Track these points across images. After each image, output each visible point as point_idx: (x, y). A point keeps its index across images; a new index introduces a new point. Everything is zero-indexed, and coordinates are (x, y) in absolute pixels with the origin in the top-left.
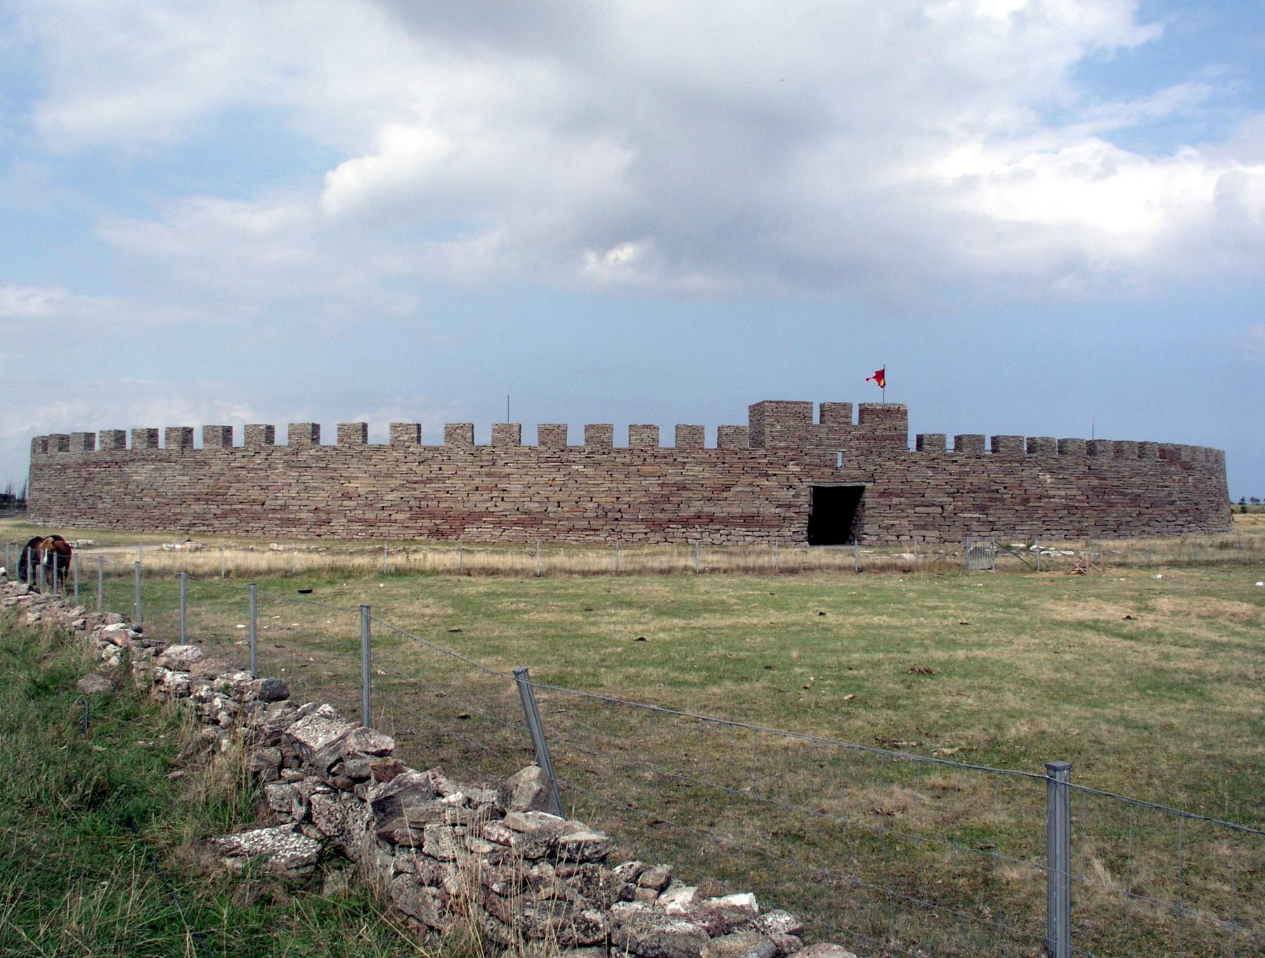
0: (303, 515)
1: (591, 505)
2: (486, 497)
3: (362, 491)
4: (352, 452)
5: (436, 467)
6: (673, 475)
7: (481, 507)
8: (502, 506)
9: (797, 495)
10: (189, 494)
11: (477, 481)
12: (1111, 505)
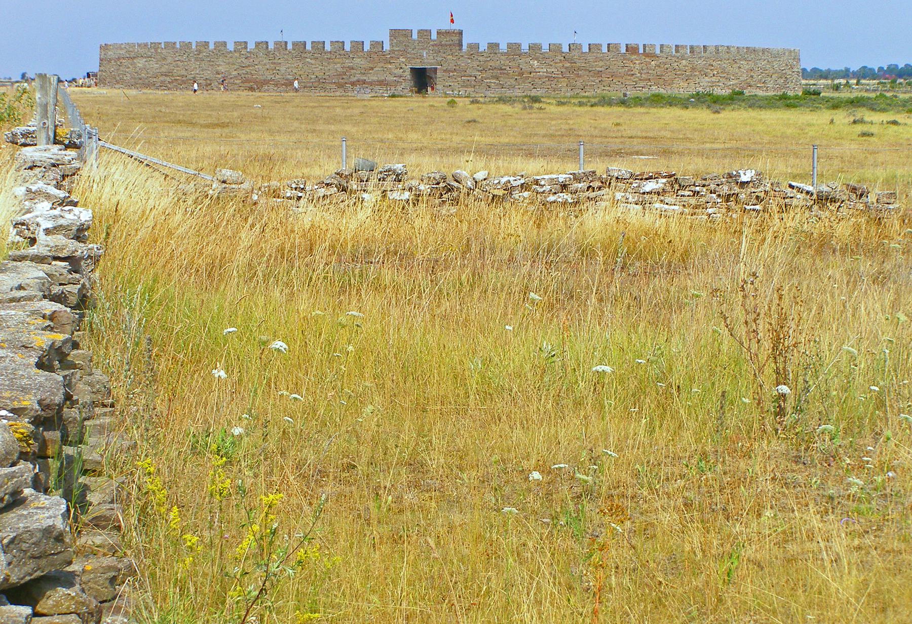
1: (313, 77)
6: (348, 63)
8: (277, 77)
9: (404, 72)
11: (268, 67)
12: (578, 76)
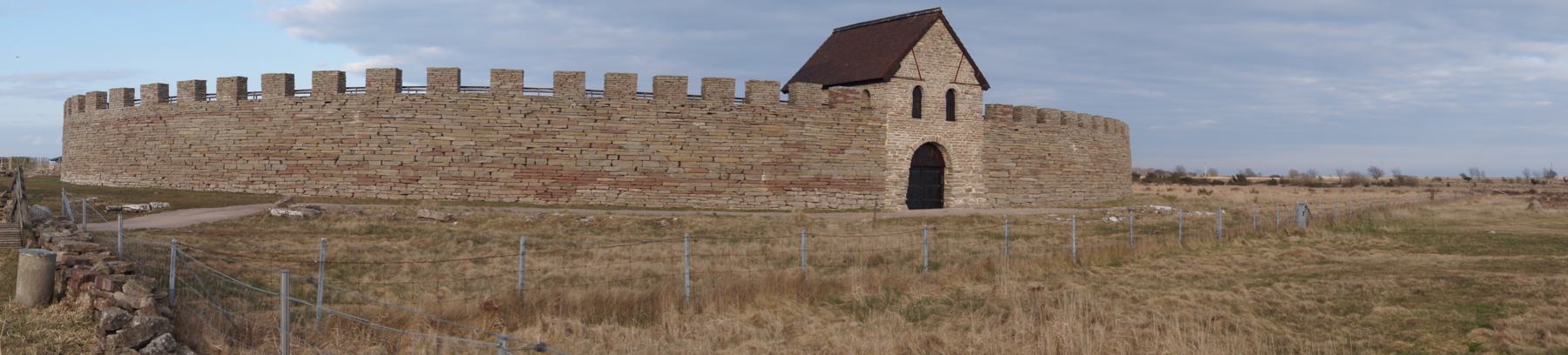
0: (387, 172)
2: (603, 155)
3: (458, 145)
4: (446, 102)
5: (544, 120)
7: (596, 166)
8: (619, 165)
10: (247, 148)
11: (591, 137)
